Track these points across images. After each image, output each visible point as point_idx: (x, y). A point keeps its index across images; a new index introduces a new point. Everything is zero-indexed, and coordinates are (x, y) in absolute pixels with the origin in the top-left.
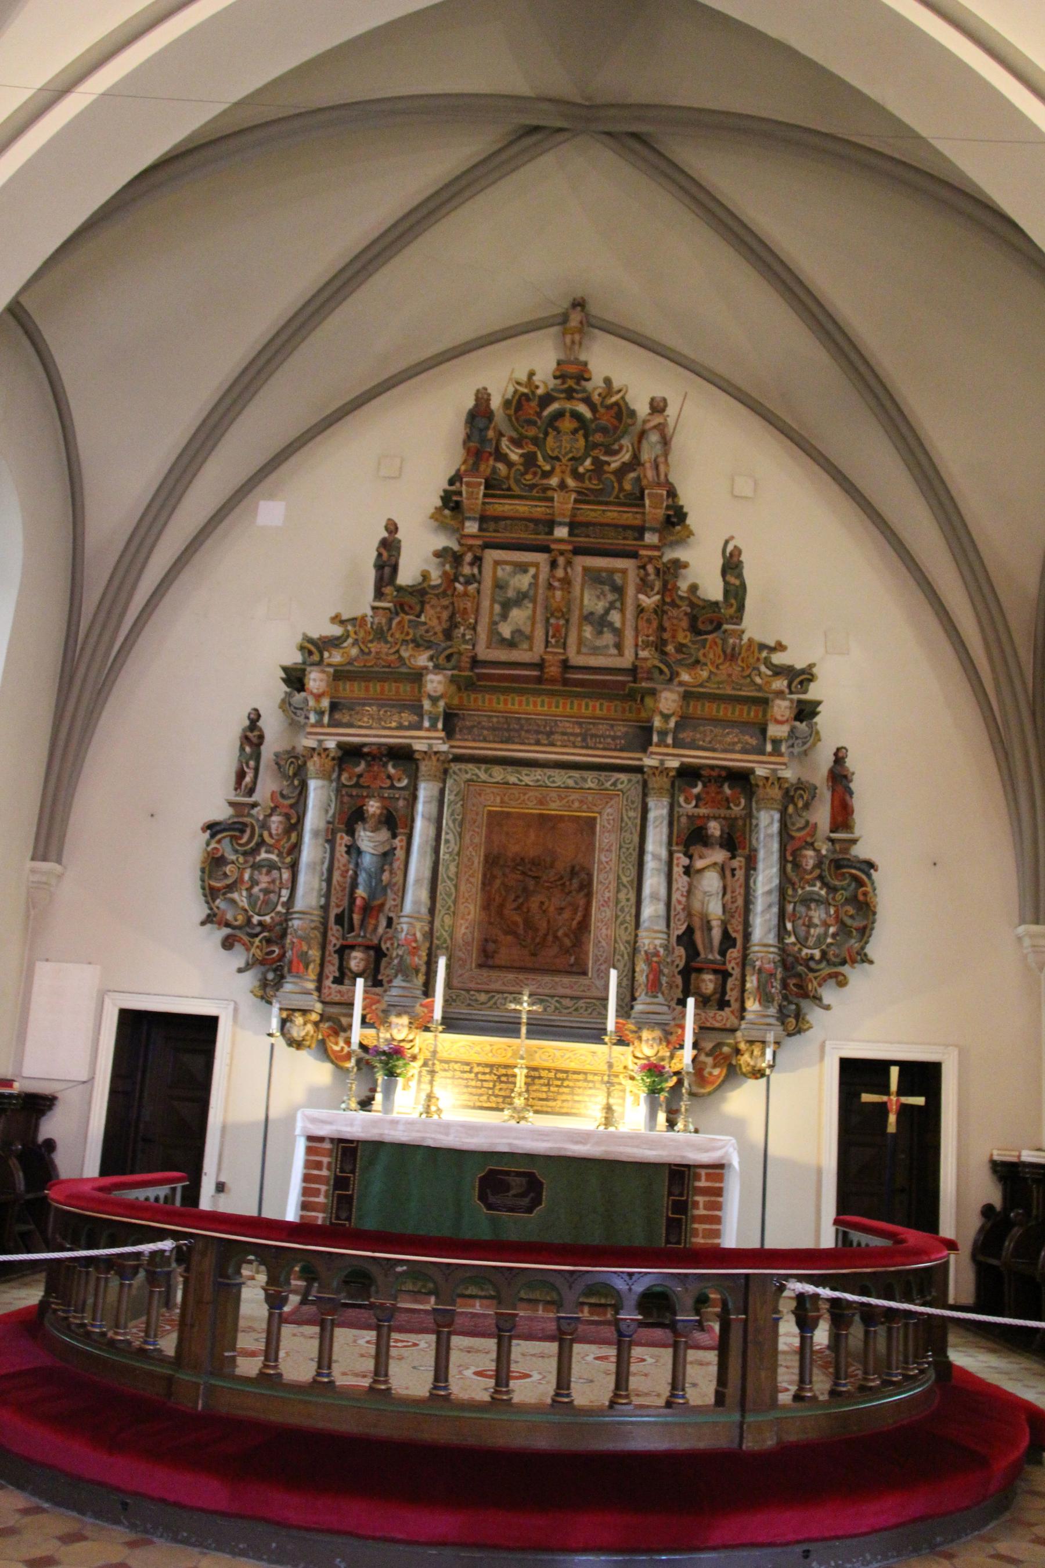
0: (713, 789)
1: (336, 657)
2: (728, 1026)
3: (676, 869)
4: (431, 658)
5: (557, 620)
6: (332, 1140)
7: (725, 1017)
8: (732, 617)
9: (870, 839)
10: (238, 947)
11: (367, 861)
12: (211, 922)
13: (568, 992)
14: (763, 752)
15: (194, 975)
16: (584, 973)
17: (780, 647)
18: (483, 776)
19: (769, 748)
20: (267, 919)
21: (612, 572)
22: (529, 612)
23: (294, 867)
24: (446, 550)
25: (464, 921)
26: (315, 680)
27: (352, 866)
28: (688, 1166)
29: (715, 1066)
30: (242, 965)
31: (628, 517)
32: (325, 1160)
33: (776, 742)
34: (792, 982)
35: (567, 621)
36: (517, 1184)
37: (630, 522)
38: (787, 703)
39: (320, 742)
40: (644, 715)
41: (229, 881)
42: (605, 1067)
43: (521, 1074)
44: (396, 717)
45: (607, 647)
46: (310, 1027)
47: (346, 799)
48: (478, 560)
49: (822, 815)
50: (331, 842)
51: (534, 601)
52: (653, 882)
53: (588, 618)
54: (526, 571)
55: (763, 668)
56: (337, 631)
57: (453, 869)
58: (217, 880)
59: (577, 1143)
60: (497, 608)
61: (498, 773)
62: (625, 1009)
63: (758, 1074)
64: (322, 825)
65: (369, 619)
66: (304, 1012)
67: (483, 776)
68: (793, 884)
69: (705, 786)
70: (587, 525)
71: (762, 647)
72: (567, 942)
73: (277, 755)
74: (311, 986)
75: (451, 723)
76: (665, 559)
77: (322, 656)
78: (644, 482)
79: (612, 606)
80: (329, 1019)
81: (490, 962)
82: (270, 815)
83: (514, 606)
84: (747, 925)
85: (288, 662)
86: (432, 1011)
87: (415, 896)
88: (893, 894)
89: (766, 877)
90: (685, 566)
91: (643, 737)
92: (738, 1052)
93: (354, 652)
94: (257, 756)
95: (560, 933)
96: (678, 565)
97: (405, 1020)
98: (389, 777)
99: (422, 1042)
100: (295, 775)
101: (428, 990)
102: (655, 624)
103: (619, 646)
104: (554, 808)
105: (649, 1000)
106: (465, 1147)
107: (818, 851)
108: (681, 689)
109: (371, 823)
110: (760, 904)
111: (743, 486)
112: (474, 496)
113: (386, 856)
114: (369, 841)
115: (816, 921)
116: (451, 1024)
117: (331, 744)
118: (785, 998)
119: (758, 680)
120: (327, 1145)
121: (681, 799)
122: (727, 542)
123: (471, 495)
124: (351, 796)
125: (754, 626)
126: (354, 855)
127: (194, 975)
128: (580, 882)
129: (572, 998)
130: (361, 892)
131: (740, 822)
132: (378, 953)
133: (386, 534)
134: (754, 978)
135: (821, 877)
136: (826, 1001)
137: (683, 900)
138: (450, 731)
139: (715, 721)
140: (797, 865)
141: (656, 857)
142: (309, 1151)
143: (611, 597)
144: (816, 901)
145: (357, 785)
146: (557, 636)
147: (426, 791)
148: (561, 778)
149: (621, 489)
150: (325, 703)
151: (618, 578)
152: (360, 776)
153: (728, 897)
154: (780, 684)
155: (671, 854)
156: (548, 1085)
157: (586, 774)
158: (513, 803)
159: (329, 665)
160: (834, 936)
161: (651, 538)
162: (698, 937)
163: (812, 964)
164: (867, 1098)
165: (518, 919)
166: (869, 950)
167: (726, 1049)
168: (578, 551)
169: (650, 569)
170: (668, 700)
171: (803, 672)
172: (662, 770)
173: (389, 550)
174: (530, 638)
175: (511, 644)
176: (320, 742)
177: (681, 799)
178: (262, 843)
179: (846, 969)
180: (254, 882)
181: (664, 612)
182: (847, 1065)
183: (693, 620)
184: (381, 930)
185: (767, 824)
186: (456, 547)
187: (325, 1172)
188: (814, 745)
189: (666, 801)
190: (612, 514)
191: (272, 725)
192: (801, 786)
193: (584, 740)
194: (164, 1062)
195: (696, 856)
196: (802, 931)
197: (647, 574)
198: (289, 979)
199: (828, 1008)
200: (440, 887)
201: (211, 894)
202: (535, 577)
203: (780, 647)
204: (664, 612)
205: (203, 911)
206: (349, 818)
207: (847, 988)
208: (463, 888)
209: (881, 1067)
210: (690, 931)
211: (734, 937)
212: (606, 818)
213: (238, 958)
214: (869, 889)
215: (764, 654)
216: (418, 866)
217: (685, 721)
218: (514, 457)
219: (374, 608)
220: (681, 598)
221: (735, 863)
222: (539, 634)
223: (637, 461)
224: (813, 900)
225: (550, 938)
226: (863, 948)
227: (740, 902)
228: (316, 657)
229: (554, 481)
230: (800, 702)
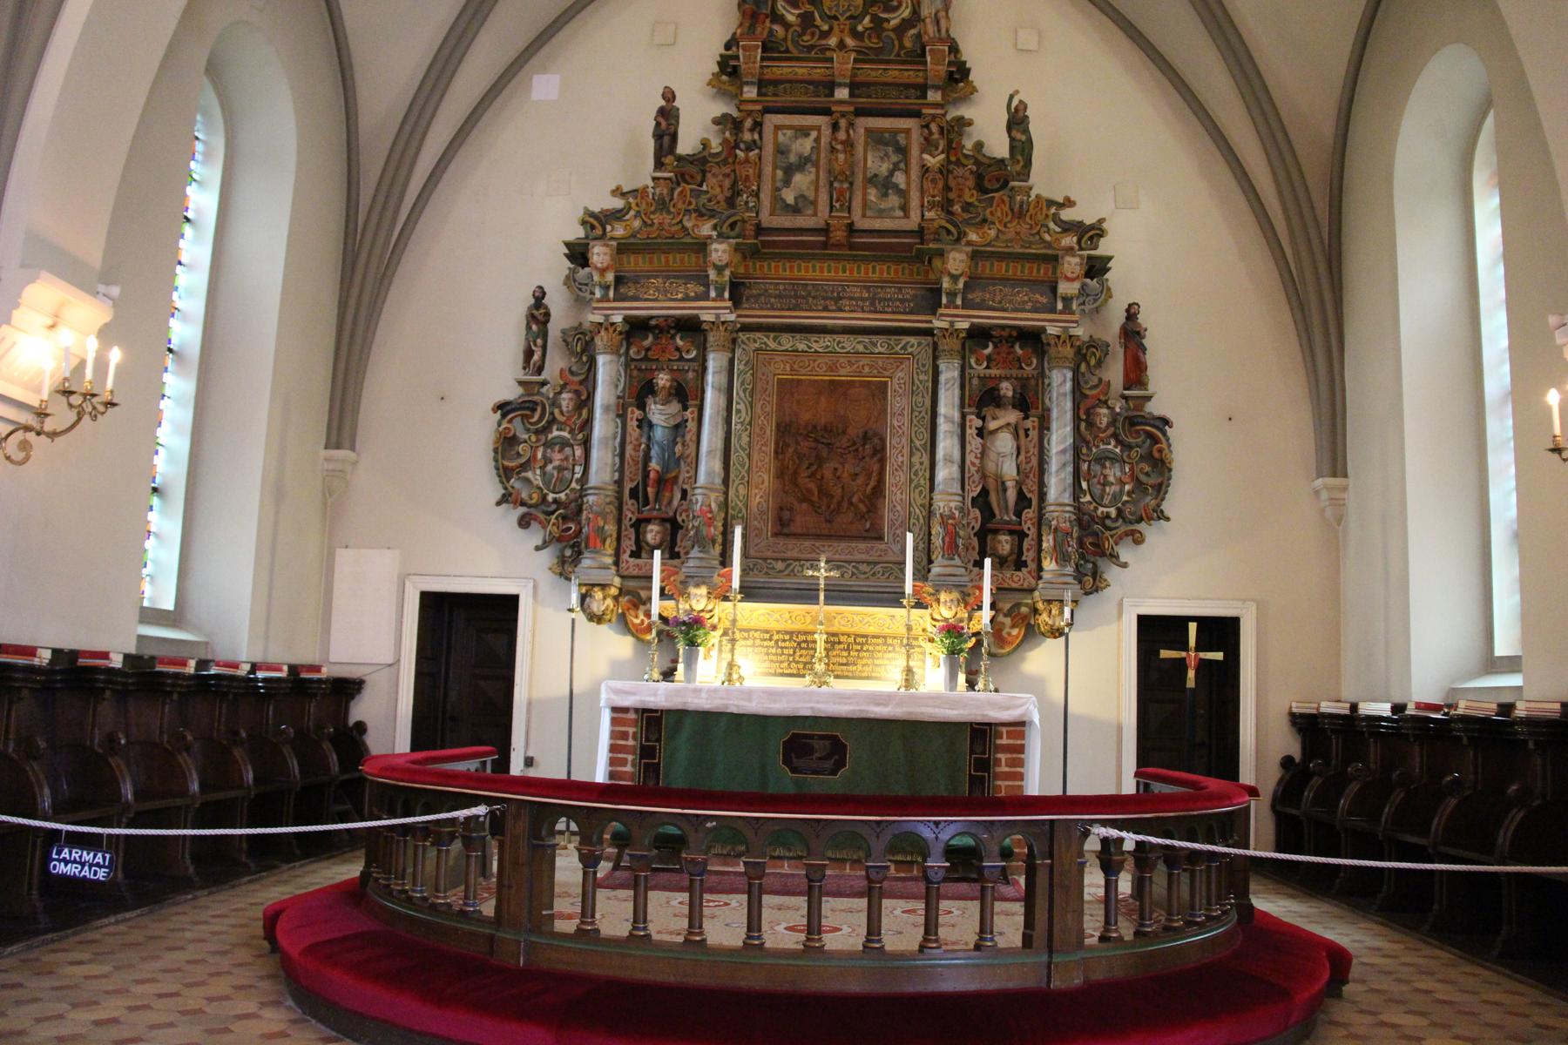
0: (1005, 349)
1: (619, 231)
2: (1025, 586)
3: (968, 431)
4: (715, 227)
5: (841, 184)
6: (636, 710)
7: (1023, 577)
8: (1018, 174)
10: (534, 525)
11: (659, 434)
12: (507, 502)
13: (863, 557)
14: (1053, 310)
15: (493, 555)
16: (881, 538)
17: (1069, 203)
18: (772, 345)
19: (1060, 306)
20: (562, 496)
21: (895, 132)
22: (813, 176)
23: (586, 444)
24: (725, 116)
25: (758, 490)
26: (599, 254)
27: (644, 440)
28: (989, 724)
29: (1013, 626)
30: (540, 543)
31: (910, 75)
32: (631, 730)
33: (1067, 300)
34: (1088, 540)
35: (851, 184)
36: (821, 747)
37: (913, 80)
38: (1077, 260)
39: (607, 317)
40: (932, 276)
41: (523, 460)
42: (903, 631)
43: (820, 640)
44: (682, 289)
45: (892, 209)
46: (609, 602)
47: (635, 373)
48: (758, 126)
49: (1114, 372)
50: (622, 416)
51: (816, 165)
52: (947, 445)
53: (872, 180)
54: (807, 135)
55: (1052, 225)
56: (618, 203)
57: (745, 439)
58: (511, 459)
59: (878, 704)
60: (780, 173)
61: (787, 341)
62: (922, 573)
63: (1057, 633)
64: (613, 400)
65: (650, 190)
66: (603, 587)
67: (772, 345)
68: (1087, 443)
69: (995, 346)
70: (868, 85)
71: (1051, 203)
72: (862, 507)
73: (564, 332)
74: (609, 560)
75: (737, 292)
76: (949, 117)
77: (604, 229)
78: (925, 38)
79: (896, 167)
80: (628, 593)
81: (786, 531)
82: (560, 393)
83: (798, 171)
84: (1042, 485)
85: (571, 238)
86: (730, 580)
87: (709, 467)
88: (1187, 449)
89: (1060, 437)
90: (970, 123)
91: (932, 299)
92: (1036, 611)
93: (637, 223)
94: (544, 334)
95: (854, 500)
96: (963, 123)
97: (703, 590)
98: (678, 349)
99: (723, 611)
100: (583, 351)
101: (725, 560)
102: (940, 184)
103: (905, 208)
104: (844, 374)
105: (946, 562)
106: (768, 713)
107: (1111, 409)
108: (970, 249)
109: (661, 396)
110: (1054, 464)
111: (1028, 39)
112: (751, 59)
113: (678, 428)
114: (660, 413)
115: (1111, 479)
116: (750, 592)
117: (618, 318)
118: (1082, 556)
119: (1047, 238)
120: (632, 716)
121: (972, 361)
122: (1011, 97)
123: (748, 59)
124: (640, 370)
125: (1043, 182)
126: (646, 429)
127: (493, 555)
128: (873, 447)
129: (869, 563)
130: (654, 465)
131: (1033, 382)
132: (673, 527)
133: (663, 103)
134: (1051, 538)
135: (1115, 436)
136: (1123, 559)
137: (977, 462)
138: (736, 301)
139: (1005, 281)
140: (1091, 424)
141: (949, 420)
142: (614, 721)
143: (894, 158)
144: (1111, 459)
145: (646, 359)
146: (841, 200)
147: (715, 363)
148: (850, 343)
149: (902, 46)
150: (610, 277)
151: (901, 138)
152: (648, 350)
153: (1022, 457)
154: (1070, 240)
155: (963, 416)
156: (848, 650)
157: (874, 338)
158: (803, 371)
159: (612, 238)
160: (1129, 494)
161: (934, 96)
162: (993, 498)
163: (1108, 522)
164: (1165, 654)
165: (812, 486)
166: (1166, 507)
167: (1024, 610)
168: (861, 112)
169: (934, 127)
170: (957, 261)
171: (1092, 227)
172: (952, 332)
173: (667, 117)
174: (814, 203)
175: (795, 210)
176: (607, 317)
177: (972, 361)
178: (553, 420)
179: (1142, 527)
180: (547, 461)
181: (949, 172)
182: (1145, 623)
183: (979, 178)
184: (675, 503)
185: (1060, 382)
186: (735, 114)
187: (631, 742)
188: (1106, 301)
189: (957, 363)
190: (894, 73)
191: (558, 302)
192: (1093, 344)
193: (872, 304)
194: (468, 641)
195: (989, 418)
196: (1097, 490)
197: (931, 133)
198: (586, 554)
199: (1125, 565)
200: (733, 457)
201: (505, 474)
202: (817, 140)
203: (1069, 203)
204: (949, 172)
205: (498, 492)
206: (640, 392)
207: (1142, 546)
208: (755, 457)
209: (1180, 623)
210: (985, 492)
211: (1030, 498)
212: (897, 381)
213: (535, 536)
214: (1164, 446)
215: (1053, 210)
216: (710, 437)
217: (973, 282)
218: (791, 18)
219: (654, 179)
220: (966, 156)
221: (1029, 424)
222: (823, 198)
223: (915, 18)
224: (1107, 458)
225: (845, 505)
226: (1159, 505)
227: (1035, 462)
228: (599, 232)
229: (833, 42)
230: (1090, 258)
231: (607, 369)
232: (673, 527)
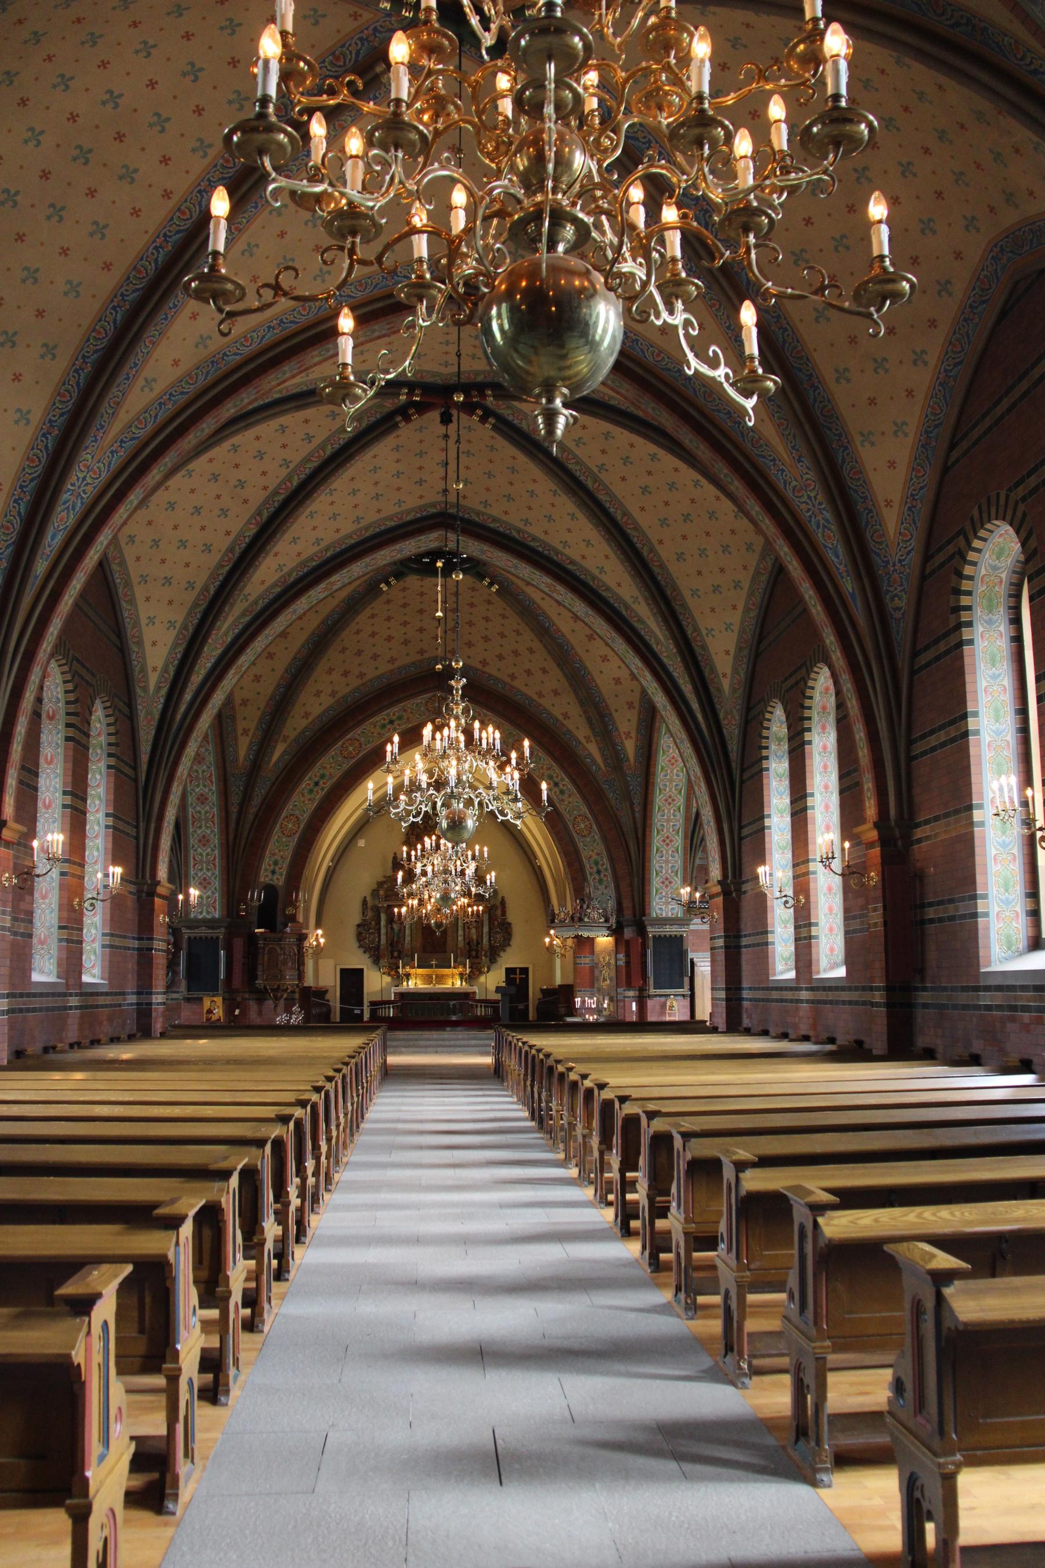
9: (512, 917)
15: (357, 960)
25: (418, 943)
26: (381, 893)
49: (499, 912)
89: (486, 929)
127: (357, 960)
132: (400, 952)
194: (352, 979)
201: (359, 941)
209: (514, 969)
211: (479, 942)
232: (400, 952)
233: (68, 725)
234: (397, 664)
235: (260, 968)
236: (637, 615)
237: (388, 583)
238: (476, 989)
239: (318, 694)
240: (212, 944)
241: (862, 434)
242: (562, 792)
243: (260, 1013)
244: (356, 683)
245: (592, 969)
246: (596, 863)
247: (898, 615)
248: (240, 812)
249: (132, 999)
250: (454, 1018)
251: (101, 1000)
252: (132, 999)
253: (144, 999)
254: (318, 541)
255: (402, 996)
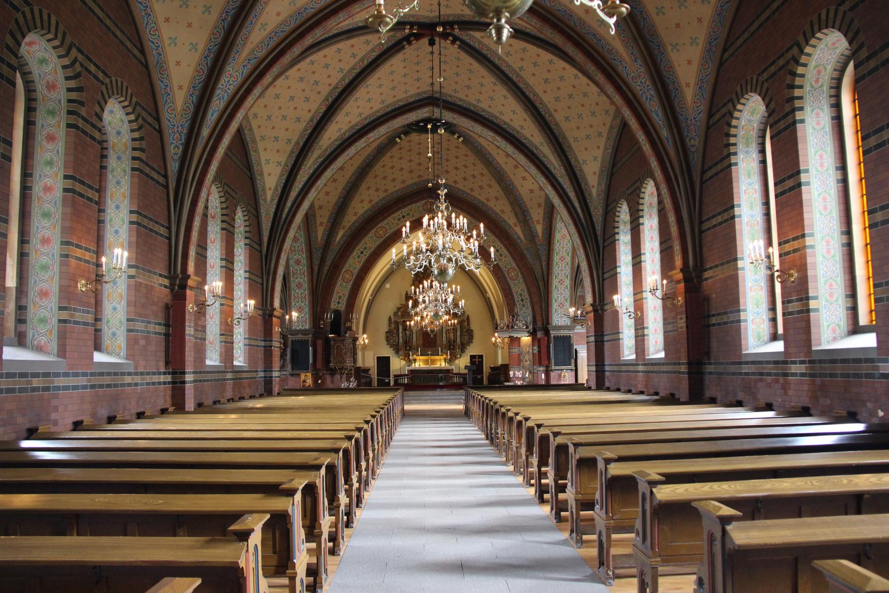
9: (474, 326)
15: (387, 352)
25: (421, 342)
49: (466, 324)
89: (459, 333)
99: (418, 358)
127: (387, 352)
132: (410, 347)
194: (384, 363)
231: (401, 327)
232: (410, 347)
233: (223, 221)
234: (406, 184)
235: (332, 357)
236: (542, 153)
237: (400, 138)
238: (453, 367)
239: (362, 202)
240: (305, 343)
241: (671, 45)
242: (501, 255)
243: (332, 382)
244: (382, 195)
245: (519, 355)
246: (521, 295)
247: (693, 149)
248: (319, 269)
249: (262, 374)
250: (441, 384)
251: (244, 375)
252: (262, 374)
253: (268, 374)
254: (360, 115)
255: (412, 372)
